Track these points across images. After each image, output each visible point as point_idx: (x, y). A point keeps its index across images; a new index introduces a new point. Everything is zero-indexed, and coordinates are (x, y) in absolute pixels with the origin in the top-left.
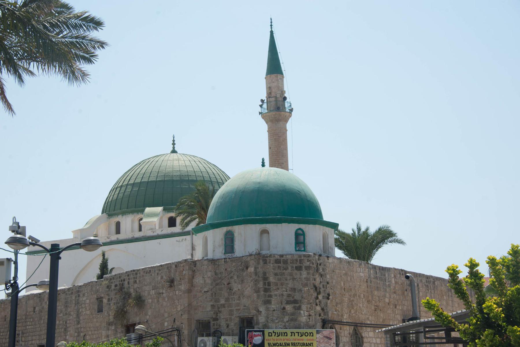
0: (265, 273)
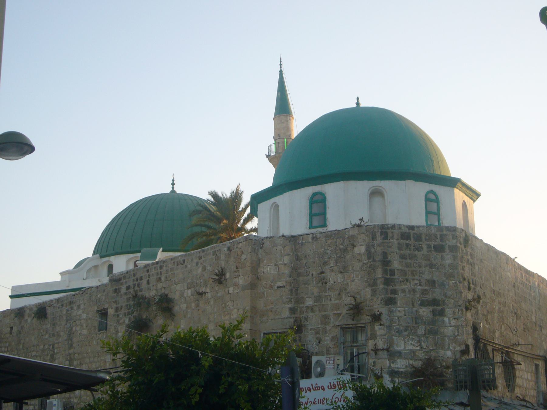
0: (385, 255)
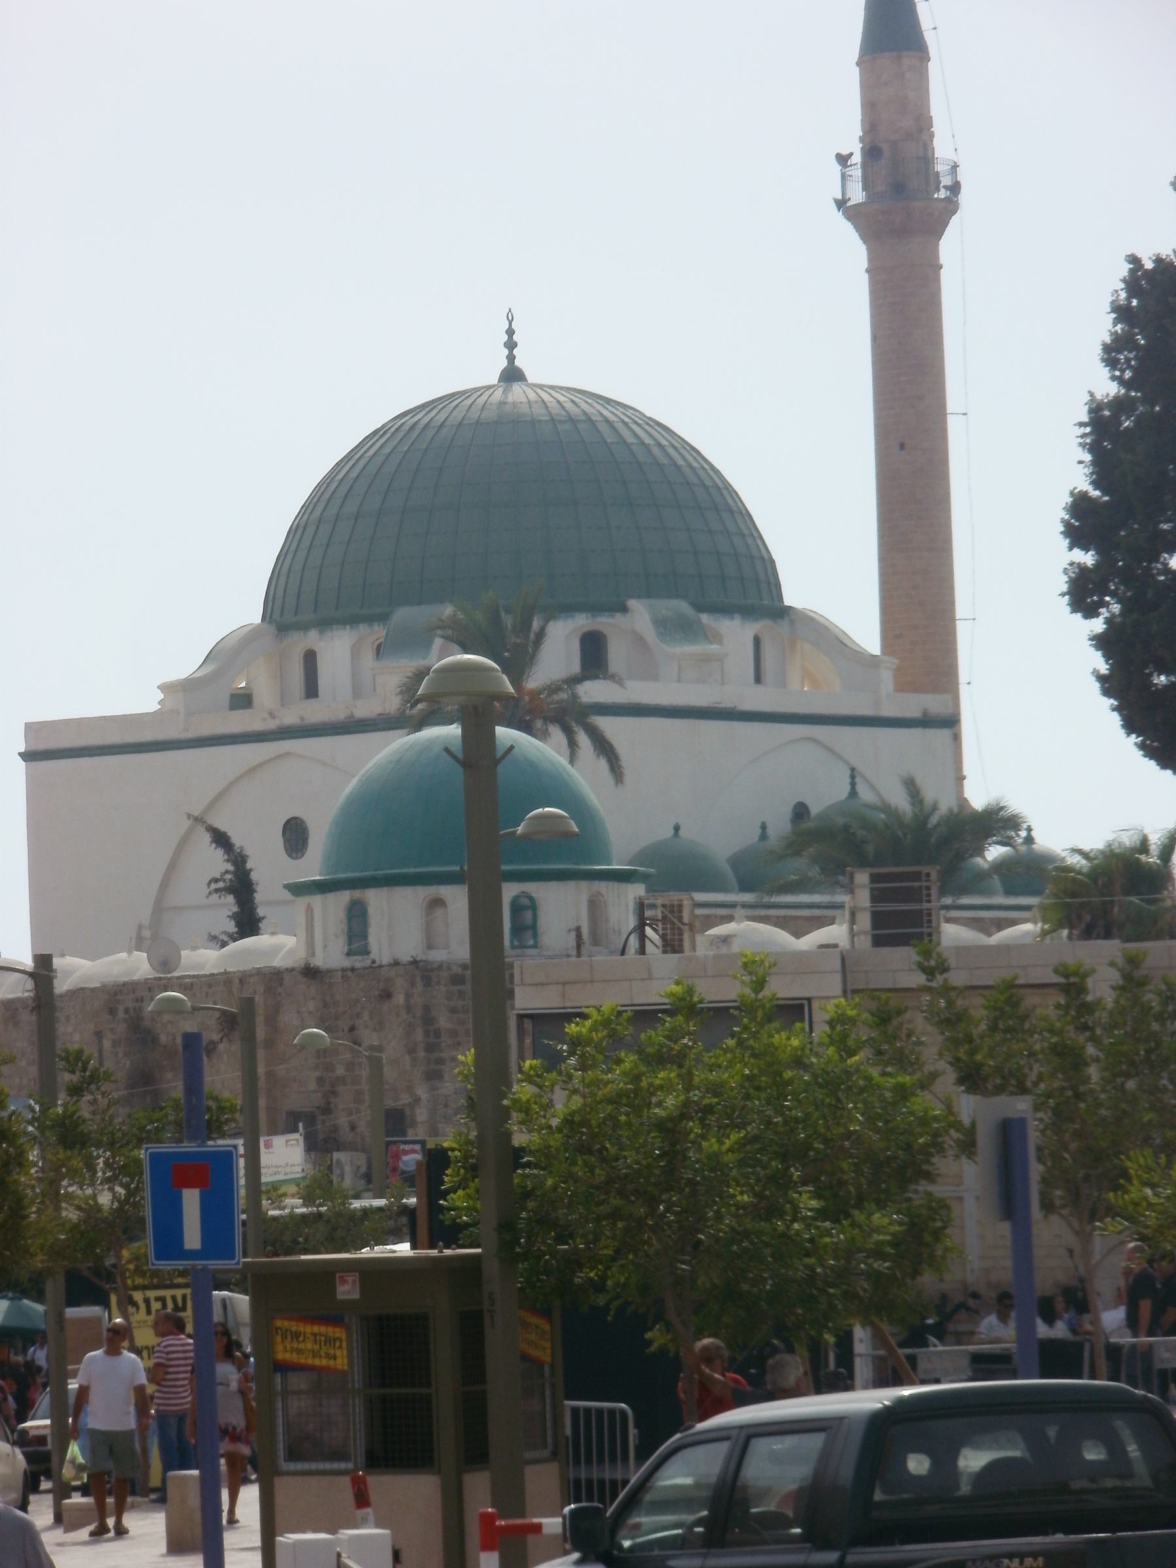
0: (427, 1009)
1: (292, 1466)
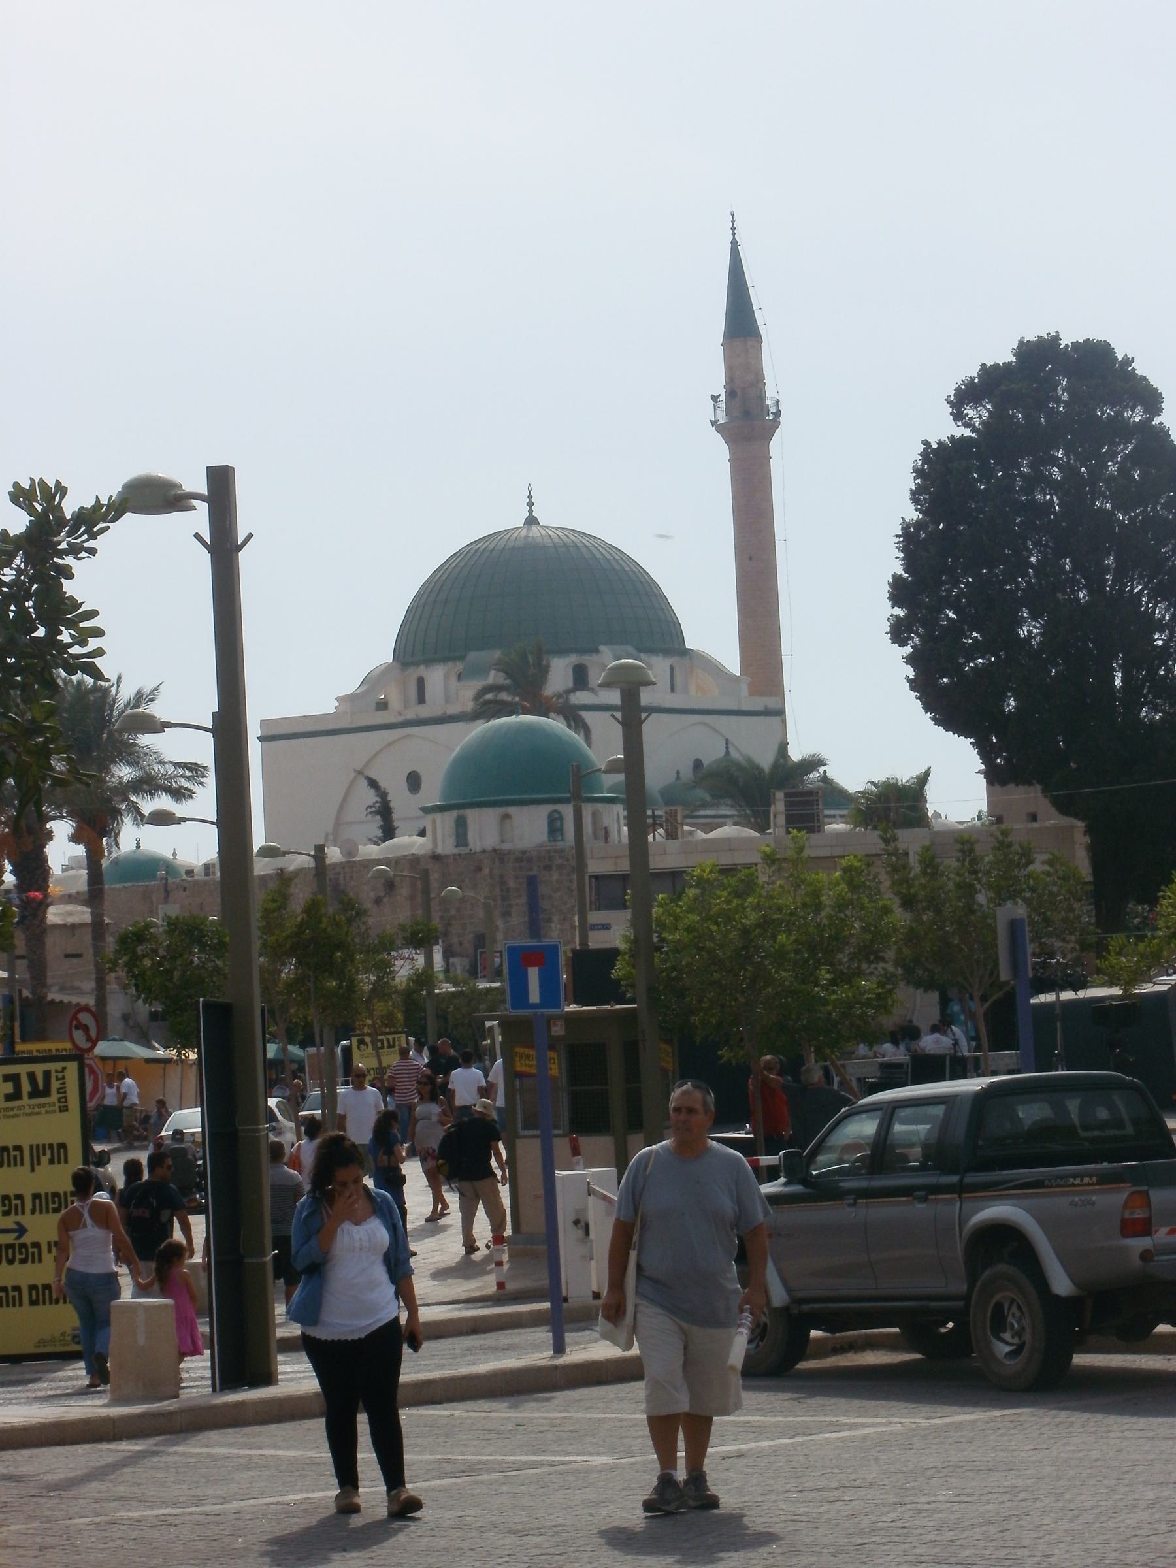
0: (502, 877)
1: (526, 1133)
